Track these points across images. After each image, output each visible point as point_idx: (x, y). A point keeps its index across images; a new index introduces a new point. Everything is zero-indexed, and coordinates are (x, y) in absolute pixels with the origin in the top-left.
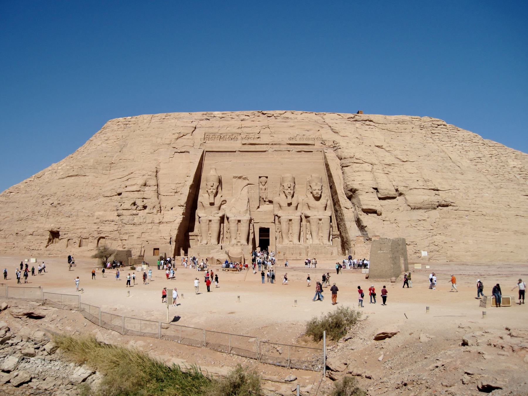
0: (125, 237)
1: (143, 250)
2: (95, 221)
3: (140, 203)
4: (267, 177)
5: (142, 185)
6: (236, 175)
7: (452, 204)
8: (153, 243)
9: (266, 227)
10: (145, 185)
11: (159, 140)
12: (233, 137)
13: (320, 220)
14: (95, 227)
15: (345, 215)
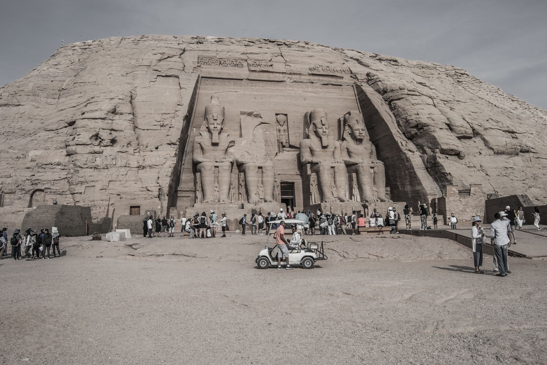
0: (80, 189)
1: (111, 208)
2: (29, 165)
3: (105, 135)
4: (286, 115)
5: (109, 112)
6: (245, 111)
7: (532, 150)
8: (128, 197)
9: (290, 181)
10: (114, 112)
11: (133, 62)
12: (237, 64)
13: (372, 168)
14: (28, 174)
15: (412, 160)
